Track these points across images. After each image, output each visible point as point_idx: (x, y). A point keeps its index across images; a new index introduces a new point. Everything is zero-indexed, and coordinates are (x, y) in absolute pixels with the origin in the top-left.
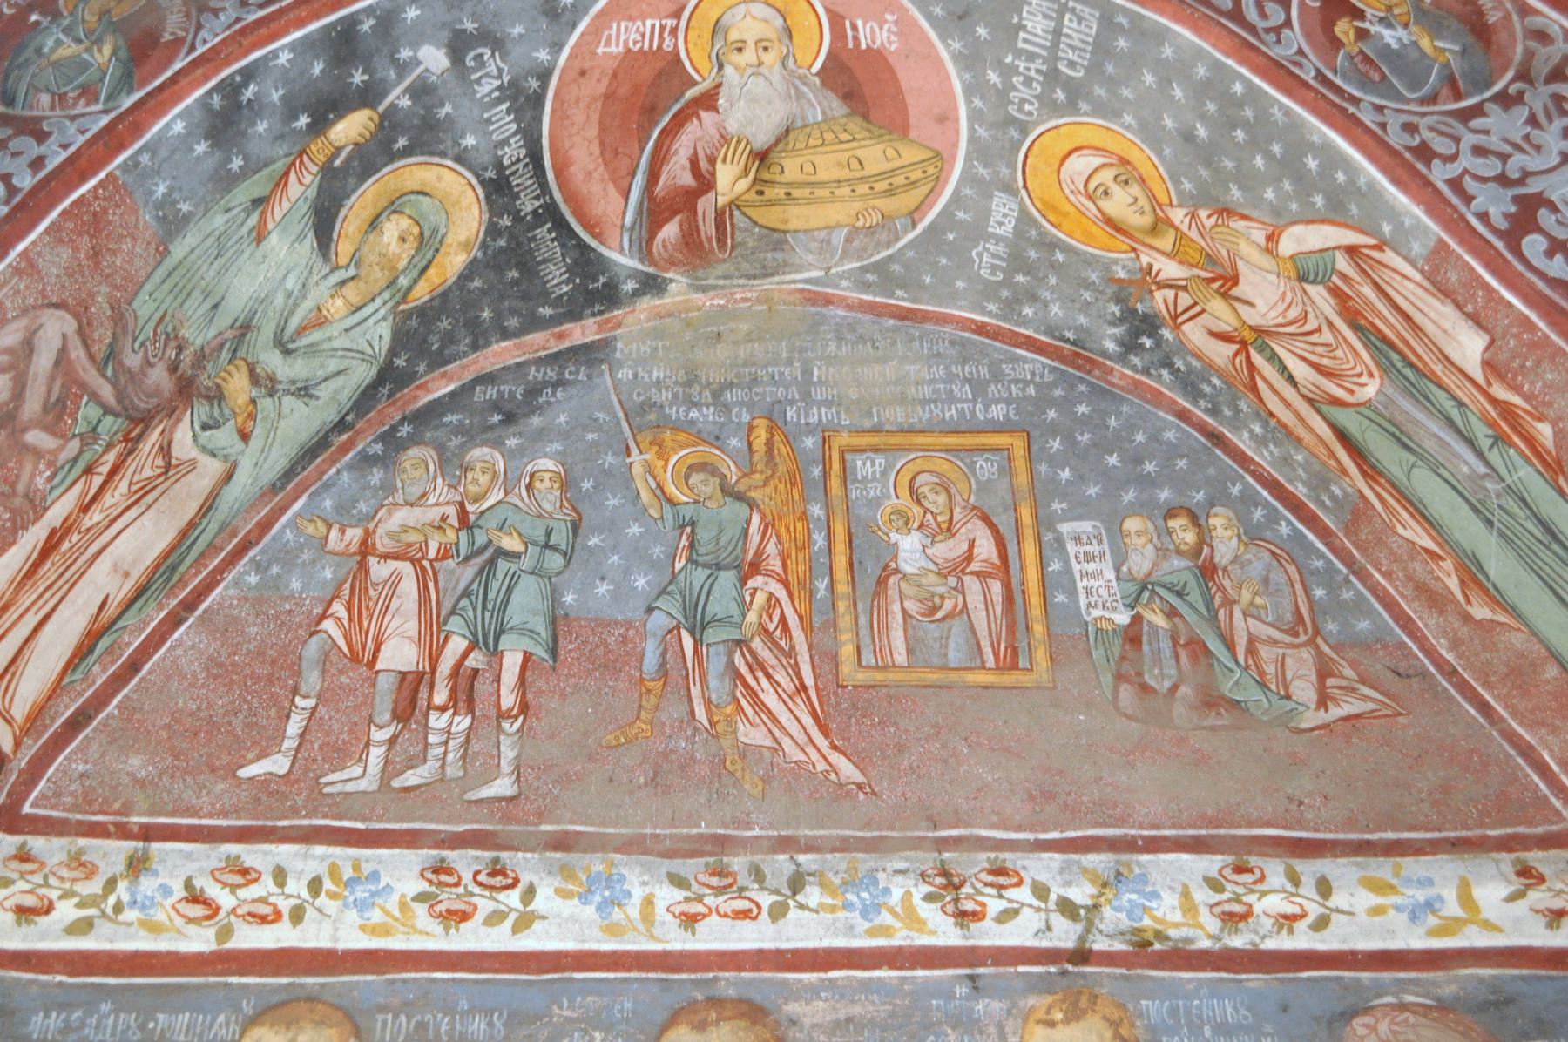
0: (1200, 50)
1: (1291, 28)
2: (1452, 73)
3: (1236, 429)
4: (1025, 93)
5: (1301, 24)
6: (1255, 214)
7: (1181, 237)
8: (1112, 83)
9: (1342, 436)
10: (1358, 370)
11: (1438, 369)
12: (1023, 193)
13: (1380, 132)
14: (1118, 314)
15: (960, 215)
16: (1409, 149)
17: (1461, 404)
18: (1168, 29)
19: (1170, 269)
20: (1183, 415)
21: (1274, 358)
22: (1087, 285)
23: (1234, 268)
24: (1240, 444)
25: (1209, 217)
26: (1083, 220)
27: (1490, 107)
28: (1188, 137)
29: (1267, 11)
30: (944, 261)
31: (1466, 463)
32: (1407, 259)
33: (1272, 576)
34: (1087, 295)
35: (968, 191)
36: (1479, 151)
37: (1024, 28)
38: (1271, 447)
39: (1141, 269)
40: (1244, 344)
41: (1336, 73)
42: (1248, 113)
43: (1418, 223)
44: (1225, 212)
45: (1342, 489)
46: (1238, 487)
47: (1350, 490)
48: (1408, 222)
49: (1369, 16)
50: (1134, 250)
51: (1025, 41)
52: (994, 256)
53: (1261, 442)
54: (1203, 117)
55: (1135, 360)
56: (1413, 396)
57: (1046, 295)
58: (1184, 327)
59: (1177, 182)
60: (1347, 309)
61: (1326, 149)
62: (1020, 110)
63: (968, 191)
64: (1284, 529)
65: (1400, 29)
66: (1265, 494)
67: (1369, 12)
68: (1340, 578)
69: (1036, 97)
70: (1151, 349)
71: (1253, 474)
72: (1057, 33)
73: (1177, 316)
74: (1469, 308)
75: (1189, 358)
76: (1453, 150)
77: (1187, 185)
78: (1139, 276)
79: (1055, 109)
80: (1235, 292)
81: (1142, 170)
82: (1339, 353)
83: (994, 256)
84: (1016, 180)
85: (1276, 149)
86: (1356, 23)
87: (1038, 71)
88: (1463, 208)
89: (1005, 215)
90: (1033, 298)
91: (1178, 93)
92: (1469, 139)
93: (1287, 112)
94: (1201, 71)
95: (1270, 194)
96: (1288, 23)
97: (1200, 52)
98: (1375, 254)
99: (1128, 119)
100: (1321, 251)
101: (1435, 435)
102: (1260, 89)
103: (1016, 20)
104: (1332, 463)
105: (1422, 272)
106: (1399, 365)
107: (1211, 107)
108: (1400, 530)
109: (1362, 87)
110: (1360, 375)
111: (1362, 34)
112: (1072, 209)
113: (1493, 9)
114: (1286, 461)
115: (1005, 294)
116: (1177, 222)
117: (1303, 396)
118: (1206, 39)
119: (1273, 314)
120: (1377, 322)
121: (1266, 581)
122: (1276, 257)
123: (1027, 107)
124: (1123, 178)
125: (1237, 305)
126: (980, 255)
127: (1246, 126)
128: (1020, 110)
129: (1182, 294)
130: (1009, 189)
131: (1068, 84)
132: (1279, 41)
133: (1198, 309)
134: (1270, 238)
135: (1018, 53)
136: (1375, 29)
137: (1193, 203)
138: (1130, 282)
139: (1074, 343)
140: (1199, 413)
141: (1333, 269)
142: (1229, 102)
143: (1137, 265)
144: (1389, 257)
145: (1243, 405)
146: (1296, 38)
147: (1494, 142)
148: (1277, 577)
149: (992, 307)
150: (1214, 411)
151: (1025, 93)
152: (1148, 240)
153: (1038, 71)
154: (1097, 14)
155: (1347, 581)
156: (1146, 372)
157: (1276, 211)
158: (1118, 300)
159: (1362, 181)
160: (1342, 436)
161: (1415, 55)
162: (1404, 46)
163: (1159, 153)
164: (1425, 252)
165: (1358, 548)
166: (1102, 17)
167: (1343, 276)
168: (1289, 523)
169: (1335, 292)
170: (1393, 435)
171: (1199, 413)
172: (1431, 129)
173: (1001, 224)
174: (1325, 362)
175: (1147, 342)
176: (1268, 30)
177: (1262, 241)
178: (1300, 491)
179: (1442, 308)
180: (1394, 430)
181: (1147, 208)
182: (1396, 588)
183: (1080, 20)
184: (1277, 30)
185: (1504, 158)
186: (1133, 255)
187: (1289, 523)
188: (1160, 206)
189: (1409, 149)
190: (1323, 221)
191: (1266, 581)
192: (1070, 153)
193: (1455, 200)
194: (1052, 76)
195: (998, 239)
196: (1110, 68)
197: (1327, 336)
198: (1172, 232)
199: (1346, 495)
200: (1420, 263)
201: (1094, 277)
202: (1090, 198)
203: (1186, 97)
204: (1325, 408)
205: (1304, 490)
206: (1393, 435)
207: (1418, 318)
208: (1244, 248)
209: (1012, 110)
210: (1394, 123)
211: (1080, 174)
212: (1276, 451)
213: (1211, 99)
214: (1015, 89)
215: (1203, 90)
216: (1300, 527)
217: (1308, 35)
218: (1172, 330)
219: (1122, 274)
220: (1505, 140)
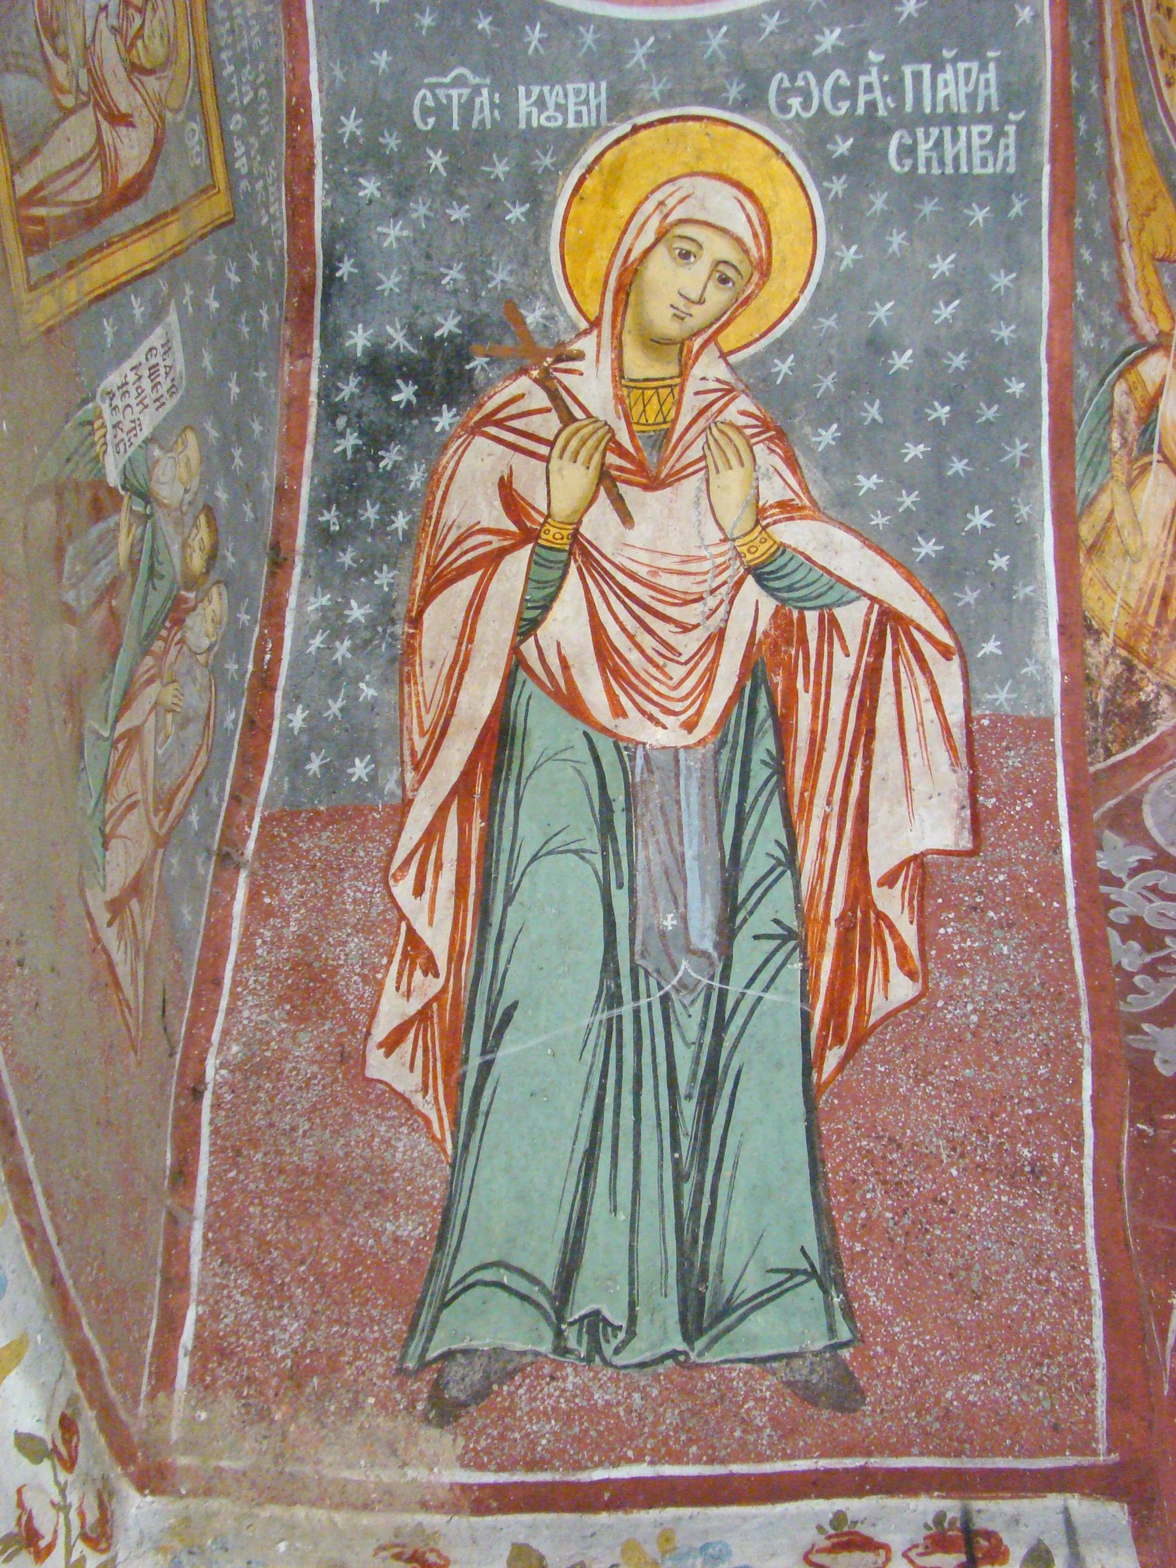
12: (626, 128)
15: (535, 35)
22: (477, 270)
23: (677, 477)
24: (293, 600)
25: (743, 413)
26: (613, 235)
30: (427, 21)
34: (454, 274)
35: (589, 38)
37: (938, 67)
51: (917, 77)
52: (467, 108)
55: (350, 387)
57: (420, 209)
62: (783, 93)
63: (589, 38)
72: (953, 119)
73: (499, 424)
78: (545, 345)
81: (764, 295)
83: (467, 108)
84: (644, 110)
87: (872, 106)
89: (562, 109)
90: (403, 192)
93: (1030, 460)
99: (849, 255)
100: (840, 579)
103: (947, 54)
112: (625, 210)
115: (392, 142)
116: (697, 371)
119: (644, 557)
123: (795, 102)
124: (730, 273)
126: (459, 82)
129: (553, 418)
130: (620, 104)
135: (891, 67)
139: (329, 279)
140: (303, 518)
143: (566, 337)
149: (351, 125)
153: (872, 106)
154: (1011, 169)
156: (331, 410)
159: (1023, 592)
163: (814, 311)
171: (303, 518)
173: (541, 103)
181: (693, 323)
182: (248, 935)
183: (993, 146)
186: (583, 325)
192: (737, 185)
195: (507, 107)
196: (928, 207)
198: (673, 370)
201: (501, 276)
209: (780, 79)
211: (703, 207)
213: (970, 356)
219: (533, 318)
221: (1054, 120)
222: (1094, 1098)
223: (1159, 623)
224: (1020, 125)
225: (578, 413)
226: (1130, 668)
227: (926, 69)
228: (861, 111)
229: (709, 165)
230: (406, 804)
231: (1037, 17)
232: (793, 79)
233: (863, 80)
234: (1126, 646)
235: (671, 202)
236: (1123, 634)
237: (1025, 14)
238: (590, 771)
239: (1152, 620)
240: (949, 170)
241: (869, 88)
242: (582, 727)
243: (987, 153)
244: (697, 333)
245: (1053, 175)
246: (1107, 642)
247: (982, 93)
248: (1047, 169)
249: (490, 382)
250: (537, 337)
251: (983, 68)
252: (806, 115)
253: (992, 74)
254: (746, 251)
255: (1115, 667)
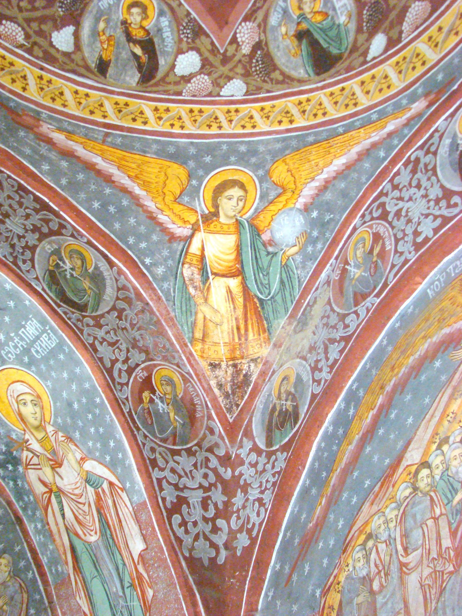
0: (91, 378)
1: (128, 387)
2: (176, 432)
3: (30, 521)
4: (12, 350)
5: (132, 386)
6: (81, 447)
7: (46, 437)
8: (50, 368)
9: (73, 549)
10: (92, 528)
11: (122, 546)
13: (142, 447)
14: (4, 450)
16: (149, 459)
17: (124, 564)
18: (83, 363)
19: (35, 446)
20: (10, 503)
21: (60, 503)
23: (62, 461)
24: (29, 528)
25: (62, 436)
26: (10, 408)
27: (183, 453)
28: (70, 405)
29: (122, 375)
31: (116, 588)
32: (130, 500)
33: (16, 597)
36: (173, 471)
37: (25, 328)
38: (41, 537)
39: (23, 439)
40: (51, 491)
41: (136, 414)
42: (97, 411)
43: (140, 491)
44: (70, 439)
45: (62, 569)
46: (19, 547)
47: (65, 572)
48: (136, 488)
49: (157, 394)
50: (25, 431)
51: (23, 332)
53: (38, 532)
54: (79, 401)
56: (108, 550)
58: (29, 470)
59: (56, 416)
60: (99, 504)
61: (118, 442)
62: (6, 354)
64: (30, 575)
65: (166, 405)
66: (29, 555)
67: (158, 392)
68: (43, 607)
69: (16, 354)
70: (11, 471)
71: (28, 543)
72: (38, 338)
73: (29, 465)
74: (144, 532)
75: (25, 483)
76: (164, 467)
77: (60, 420)
78: (21, 441)
79: (21, 363)
80: (58, 469)
81: (44, 404)
82: (88, 517)
85: (101, 430)
86: (151, 395)
87: (22, 346)
88: (158, 493)
91: (74, 387)
92: (172, 464)
93: (112, 420)
94: (87, 385)
95: (90, 444)
96: (127, 384)
97: (90, 379)
98: (119, 491)
99: (49, 383)
100: (100, 476)
101: (110, 571)
102: (106, 406)
104: (63, 557)
105: (133, 509)
106: (109, 536)
107: (84, 400)
108: (78, 598)
109: (143, 424)
110: (92, 531)
111: (152, 401)
112: (7, 401)
113: (200, 411)
114: (44, 545)
116: (48, 431)
117: (65, 524)
118: (94, 376)
119: (69, 487)
120: (108, 515)
121: (12, 598)
122: (81, 467)
123: (10, 355)
124: (35, 402)
125: (56, 475)
127: (94, 414)
128: (6, 354)
131: (31, 358)
132: (121, 390)
133: (39, 467)
134: (82, 459)
135: (17, 335)
136: (157, 401)
137: (58, 428)
138: (16, 441)
140: (18, 506)
141: (101, 486)
142: (91, 401)
143: (23, 437)
144: (124, 495)
145: (38, 513)
146: (127, 392)
147: (179, 469)
148: (18, 597)
150: (25, 509)
151: (12, 350)
152: (32, 430)
153: (22, 346)
154: (58, 341)
155: (45, 609)
157: (90, 451)
158: (7, 445)
159: (127, 462)
160: (73, 549)
161: (166, 418)
162: (164, 412)
163: (55, 403)
164: (138, 502)
165: (57, 597)
166: (59, 343)
167: (103, 491)
168: (33, 573)
169: (97, 494)
170: (93, 561)
171: (18, 506)
172: (160, 454)
174: (80, 517)
175: (10, 467)
176: (119, 383)
177: (79, 459)
178: (44, 560)
179: (134, 526)
180: (95, 559)
181: (39, 419)
183: (50, 339)
184: (122, 385)
185: (180, 477)
186: (23, 432)
187: (33, 573)
188: (45, 421)
189: (149, 459)
190: (106, 466)
191: (12, 598)
193: (157, 488)
194: (27, 351)
196: (52, 362)
197: (86, 508)
199: (63, 572)
200: (134, 505)
202: (17, 402)
203: (76, 391)
204: (71, 534)
205: (46, 561)
206: (93, 561)
207: (124, 523)
208: (70, 456)
210: (149, 445)
212: (42, 539)
213: (85, 398)
214: (9, 346)
215: (85, 392)
216: (37, 576)
217: (132, 392)
218: (24, 469)
219: (14, 437)
220: (183, 470)
221: (55, 322)
222: (187, 609)
223: (240, 339)
224: (50, 329)
225: (39, 454)
226: (235, 366)
227: (23, 329)
228: (22, 349)
229: (10, 382)
230: (69, 575)
231: (30, 301)
232: (5, 351)
233: (15, 341)
234: (233, 359)
235: (12, 394)
236: (229, 356)
237: (27, 303)
238: (88, 553)
239: (237, 340)
240: (48, 351)
241: (19, 343)
242: (82, 542)
243: (50, 341)
244: (41, 421)
245: (66, 335)
246: (223, 365)
247: (37, 327)
248: (64, 335)
249: (20, 456)
250: (18, 440)
251: (33, 321)
252: (14, 357)
253: (35, 321)
254: (33, 395)
255: (230, 370)
